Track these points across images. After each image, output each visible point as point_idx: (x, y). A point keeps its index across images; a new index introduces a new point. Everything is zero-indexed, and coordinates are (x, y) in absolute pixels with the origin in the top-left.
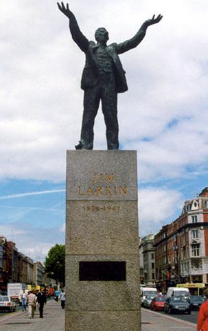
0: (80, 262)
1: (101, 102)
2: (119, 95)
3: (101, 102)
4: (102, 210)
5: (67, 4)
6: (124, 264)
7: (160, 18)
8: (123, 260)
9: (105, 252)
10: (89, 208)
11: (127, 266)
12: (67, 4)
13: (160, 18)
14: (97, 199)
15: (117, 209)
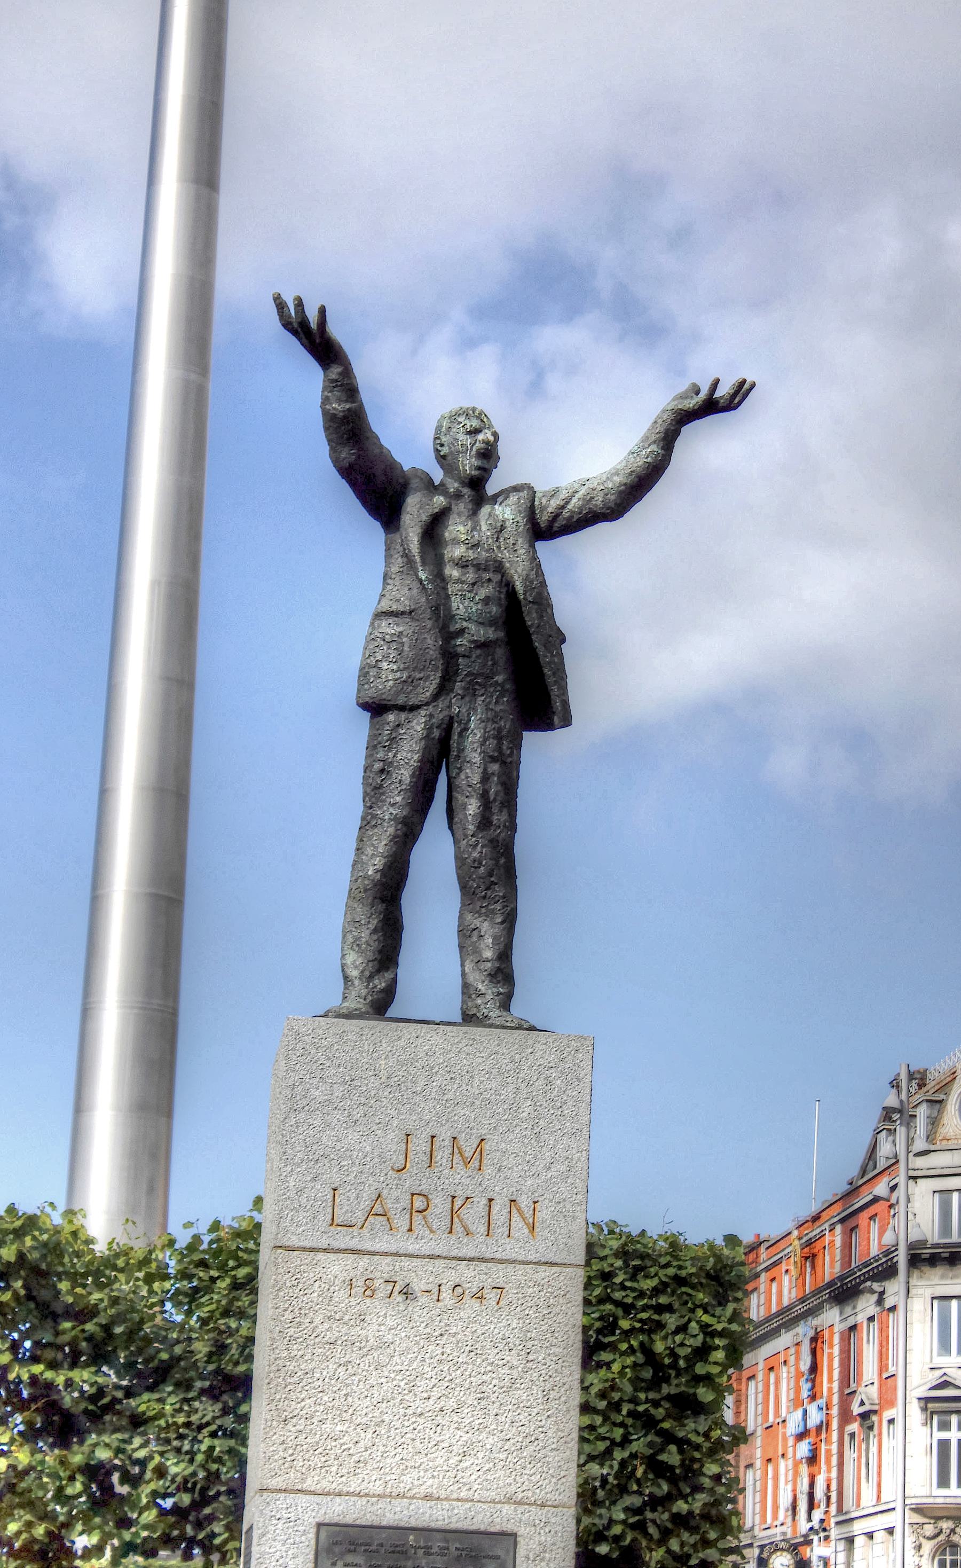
0: (319, 1525)
1: (444, 763)
2: (532, 740)
3: (444, 763)
4: (424, 1299)
5: (322, 311)
6: (512, 1537)
7: (742, 391)
8: (509, 1527)
9: (430, 1485)
10: (369, 1291)
11: (521, 1552)
12: (322, 311)
13: (742, 391)
14: (412, 1248)
15: (492, 1296)
